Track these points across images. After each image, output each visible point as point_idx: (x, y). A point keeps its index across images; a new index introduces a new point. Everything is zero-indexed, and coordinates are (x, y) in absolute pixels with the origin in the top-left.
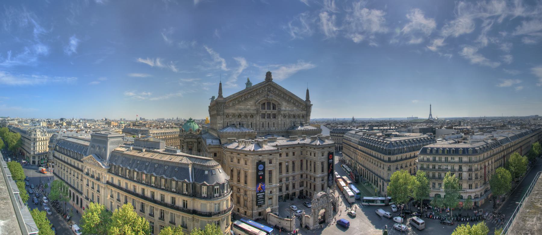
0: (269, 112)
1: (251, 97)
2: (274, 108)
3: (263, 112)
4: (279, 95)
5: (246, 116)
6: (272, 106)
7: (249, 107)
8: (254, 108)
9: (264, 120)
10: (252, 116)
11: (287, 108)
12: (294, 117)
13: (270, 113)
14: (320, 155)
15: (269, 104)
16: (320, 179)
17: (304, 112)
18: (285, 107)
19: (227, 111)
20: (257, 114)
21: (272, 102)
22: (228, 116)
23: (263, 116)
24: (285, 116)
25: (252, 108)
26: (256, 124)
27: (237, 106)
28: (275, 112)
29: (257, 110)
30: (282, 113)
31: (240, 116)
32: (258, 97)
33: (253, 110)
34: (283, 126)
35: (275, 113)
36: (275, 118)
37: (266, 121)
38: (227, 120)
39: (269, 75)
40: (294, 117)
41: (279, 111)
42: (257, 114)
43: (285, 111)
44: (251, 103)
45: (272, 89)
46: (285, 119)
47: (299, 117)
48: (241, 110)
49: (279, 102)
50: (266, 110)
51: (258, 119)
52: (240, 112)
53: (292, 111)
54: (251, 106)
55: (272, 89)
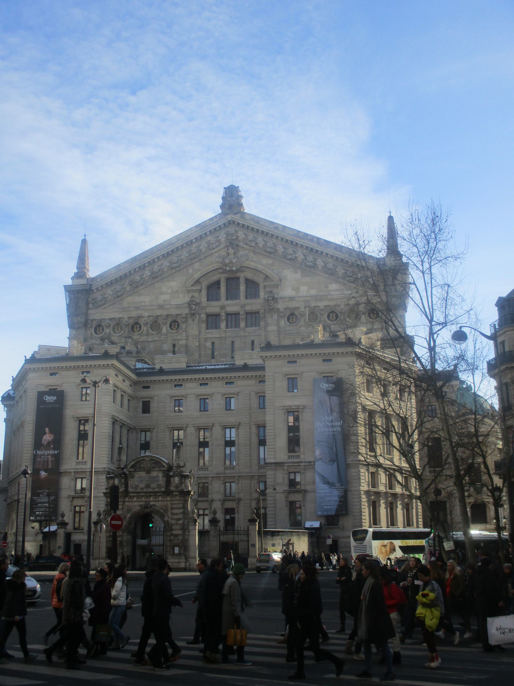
0: (232, 306)
3: (214, 307)
5: (155, 325)
6: (242, 288)
7: (167, 297)
9: (214, 334)
15: (232, 281)
19: (96, 315)
21: (242, 276)
22: (99, 327)
23: (212, 320)
25: (174, 302)
26: (186, 346)
27: (130, 300)
28: (255, 305)
30: (281, 306)
31: (135, 325)
32: (197, 266)
33: (178, 307)
36: (256, 324)
43: (292, 299)
45: (241, 234)
48: (137, 308)
49: (268, 272)
50: (223, 301)
52: (134, 314)
55: (241, 234)
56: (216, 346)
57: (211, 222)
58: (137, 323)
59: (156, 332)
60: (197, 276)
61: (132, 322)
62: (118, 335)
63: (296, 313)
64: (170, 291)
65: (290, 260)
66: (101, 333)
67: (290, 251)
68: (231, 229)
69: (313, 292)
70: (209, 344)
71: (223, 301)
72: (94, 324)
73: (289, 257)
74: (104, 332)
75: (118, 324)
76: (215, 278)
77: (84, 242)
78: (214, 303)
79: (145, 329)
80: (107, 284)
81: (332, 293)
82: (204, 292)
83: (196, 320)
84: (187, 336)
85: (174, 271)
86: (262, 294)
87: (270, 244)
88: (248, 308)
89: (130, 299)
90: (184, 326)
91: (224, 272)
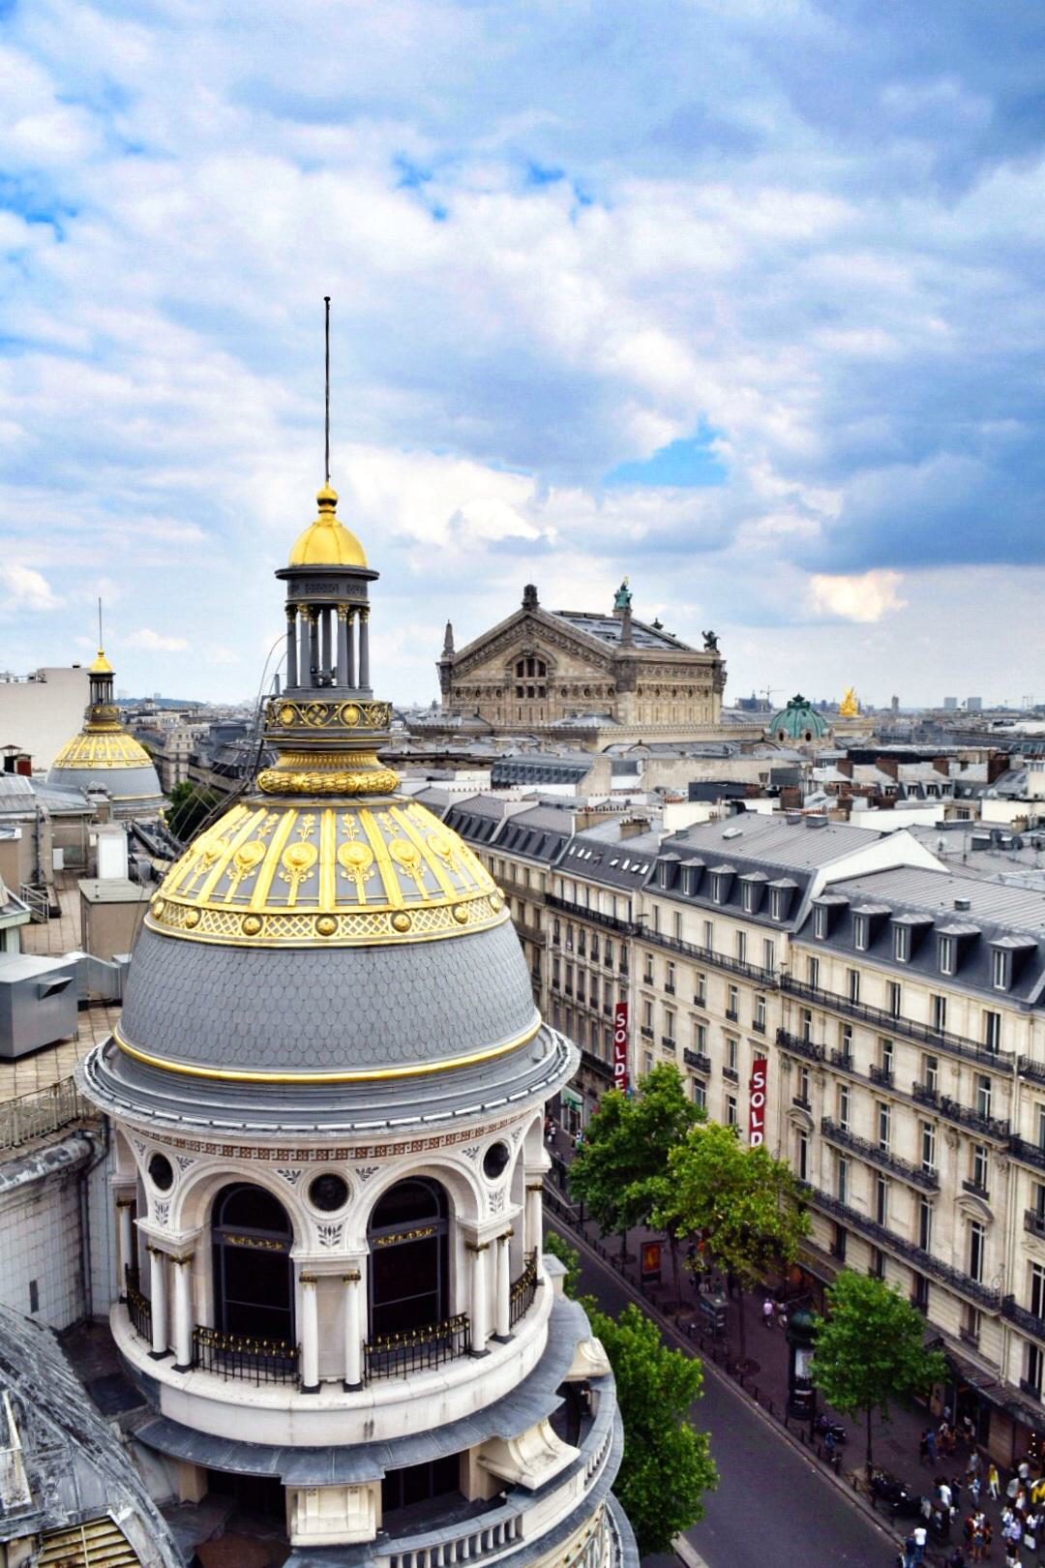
2: (542, 673)
5: (488, 691)
6: (536, 668)
8: (501, 675)
9: (521, 702)
10: (499, 693)
15: (531, 662)
23: (520, 692)
24: (564, 692)
28: (542, 681)
30: (557, 683)
31: (478, 693)
37: (525, 700)
39: (530, 592)
40: (587, 691)
47: (599, 690)
50: (525, 678)
53: (579, 679)
71: (525, 678)
77: (449, 626)
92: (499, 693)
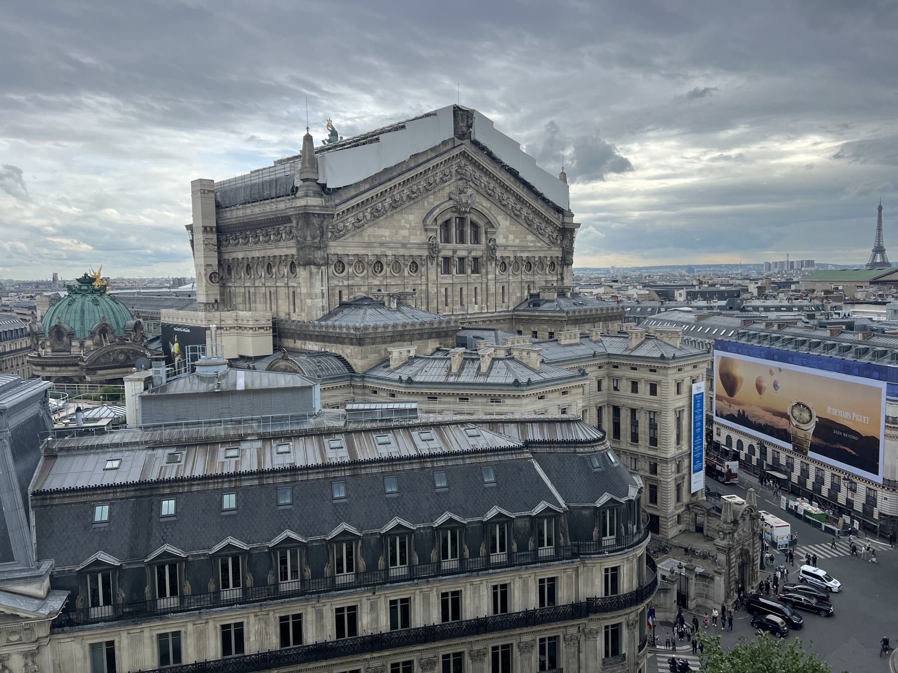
1: (409, 198)
4: (489, 196)
6: (468, 230)
7: (405, 233)
8: (420, 238)
9: (447, 279)
10: (415, 267)
11: (511, 237)
12: (529, 265)
13: (463, 253)
14: (673, 389)
16: (673, 467)
17: (557, 252)
18: (509, 235)
19: (336, 248)
20: (431, 258)
21: (469, 217)
22: (340, 264)
24: (504, 266)
28: (479, 251)
29: (433, 249)
30: (498, 254)
32: (431, 198)
33: (420, 246)
34: (500, 298)
35: (478, 254)
38: (339, 282)
41: (492, 249)
42: (431, 258)
44: (411, 217)
46: (504, 277)
48: (382, 244)
50: (453, 245)
51: (432, 276)
52: (378, 251)
53: (523, 249)
54: (412, 229)
56: (449, 293)
57: (445, 149)
58: (379, 262)
59: (397, 275)
60: (436, 213)
61: (374, 259)
62: (361, 275)
63: (507, 261)
64: (408, 226)
65: (504, 206)
66: (342, 272)
67: (505, 196)
68: (463, 162)
69: (517, 242)
70: (443, 290)
72: (335, 259)
73: (504, 203)
74: (346, 271)
75: (360, 261)
76: (448, 216)
78: (448, 246)
79: (388, 270)
80: (348, 210)
81: (530, 244)
82: (439, 232)
83: (435, 264)
84: (427, 280)
85: (412, 202)
86: (483, 239)
87: (491, 186)
88: (473, 254)
89: (370, 230)
90: (423, 269)
91: (458, 211)
92: (415, 267)
